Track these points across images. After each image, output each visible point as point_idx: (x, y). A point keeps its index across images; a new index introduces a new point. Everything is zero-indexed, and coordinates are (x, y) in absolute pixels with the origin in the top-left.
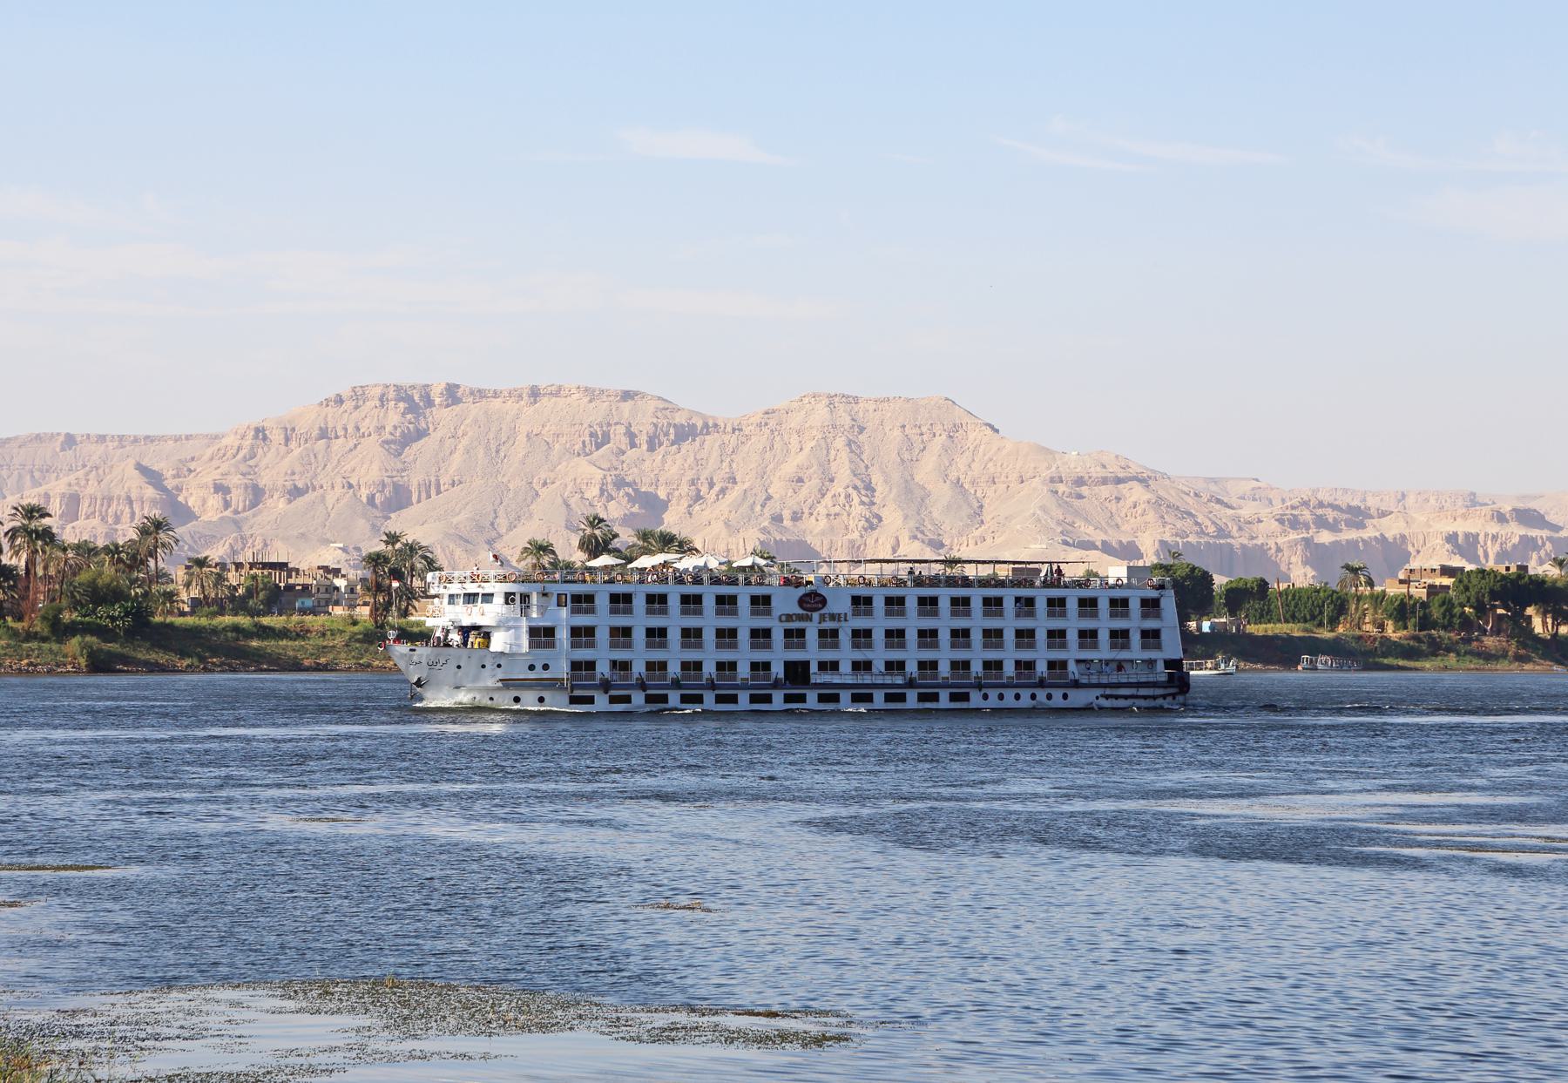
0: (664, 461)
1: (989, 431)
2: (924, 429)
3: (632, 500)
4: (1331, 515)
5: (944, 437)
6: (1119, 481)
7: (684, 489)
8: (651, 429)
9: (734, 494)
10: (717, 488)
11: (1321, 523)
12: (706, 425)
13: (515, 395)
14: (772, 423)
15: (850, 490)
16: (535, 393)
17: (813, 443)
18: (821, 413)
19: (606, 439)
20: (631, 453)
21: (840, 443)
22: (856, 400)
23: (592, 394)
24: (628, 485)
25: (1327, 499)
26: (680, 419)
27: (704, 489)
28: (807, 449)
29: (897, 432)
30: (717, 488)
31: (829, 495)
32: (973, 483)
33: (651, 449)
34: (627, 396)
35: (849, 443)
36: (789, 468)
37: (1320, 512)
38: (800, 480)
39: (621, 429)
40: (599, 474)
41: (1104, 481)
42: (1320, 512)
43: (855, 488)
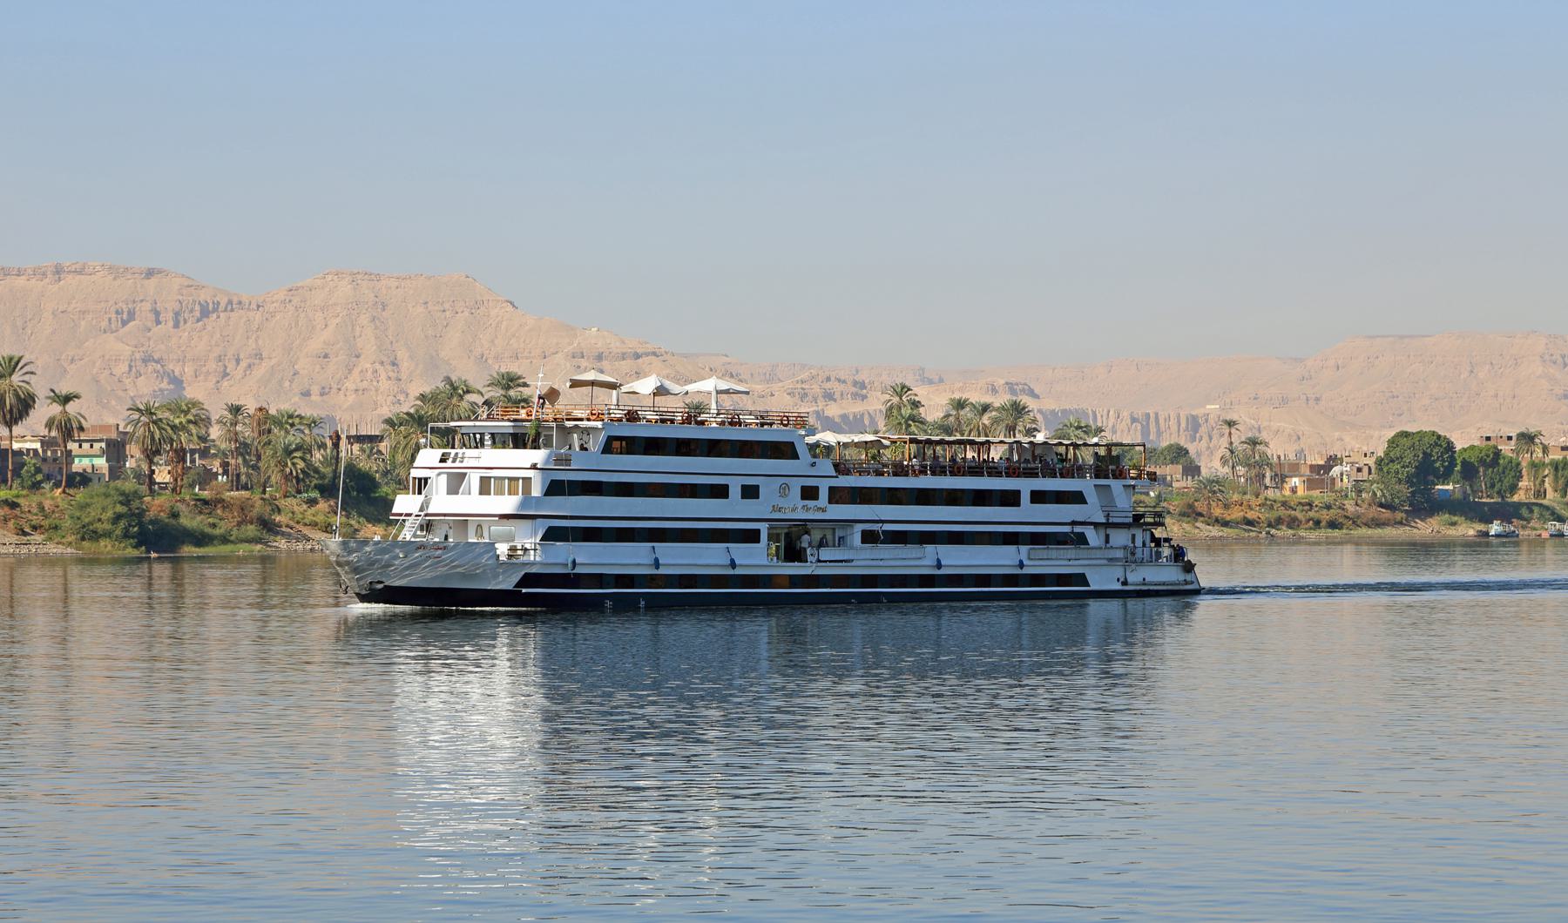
0: (190, 338)
1: (510, 308)
2: (447, 306)
3: (160, 375)
4: (837, 388)
5: (466, 314)
6: (637, 356)
7: (212, 365)
8: (177, 306)
9: (260, 371)
10: (243, 364)
11: (829, 396)
12: (230, 302)
13: (39, 273)
14: (296, 300)
15: (377, 366)
16: (58, 271)
17: (338, 320)
18: (345, 289)
19: (132, 315)
20: (156, 329)
21: (364, 319)
22: (378, 277)
23: (116, 272)
24: (157, 362)
25: (833, 375)
26: (203, 296)
27: (231, 367)
28: (331, 327)
29: (420, 309)
30: (243, 364)
31: (356, 371)
32: (496, 358)
33: (176, 326)
34: (150, 273)
35: (373, 319)
36: (316, 345)
37: (828, 385)
38: (326, 356)
39: (147, 306)
40: (127, 350)
41: (623, 357)
42: (828, 385)
43: (382, 363)
